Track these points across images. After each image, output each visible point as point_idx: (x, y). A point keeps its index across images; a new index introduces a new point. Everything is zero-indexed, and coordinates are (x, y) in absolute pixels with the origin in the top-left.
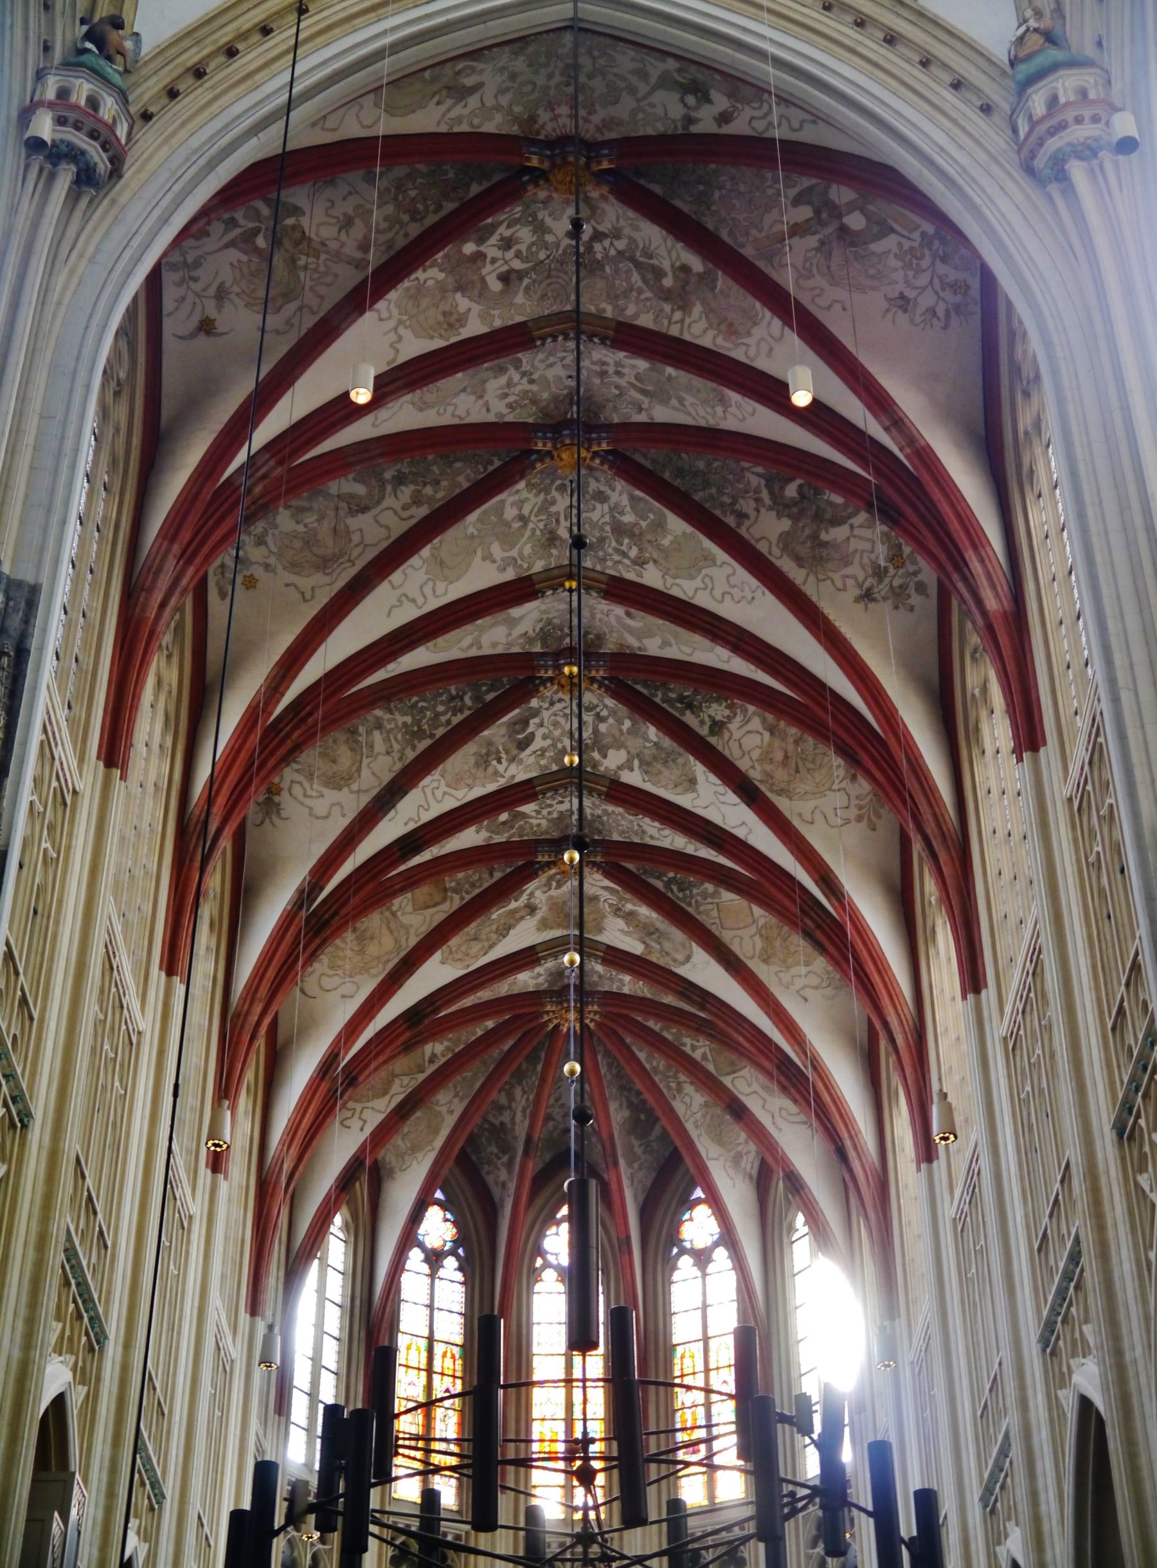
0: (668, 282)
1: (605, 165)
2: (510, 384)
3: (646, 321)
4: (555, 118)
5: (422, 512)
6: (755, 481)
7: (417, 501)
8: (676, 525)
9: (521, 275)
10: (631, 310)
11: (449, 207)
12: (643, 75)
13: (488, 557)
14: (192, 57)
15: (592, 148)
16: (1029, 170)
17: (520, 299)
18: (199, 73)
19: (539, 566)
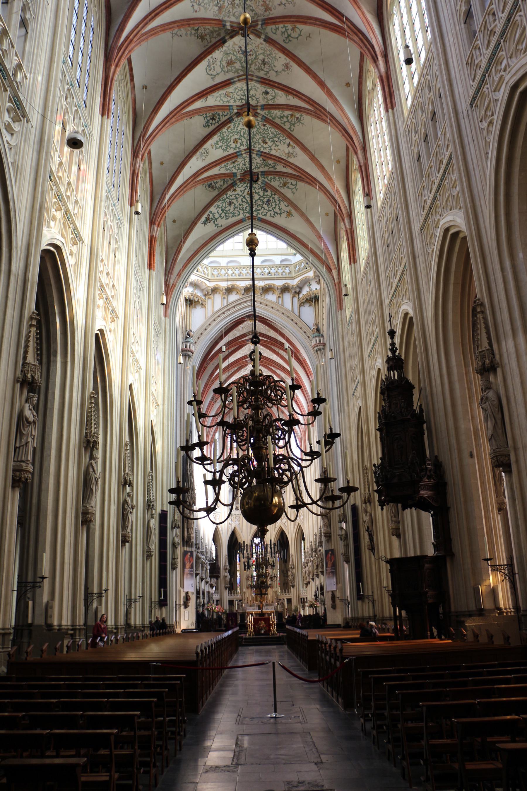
3: (264, 332)
14: (200, 332)
17: (245, 330)
18: (202, 334)
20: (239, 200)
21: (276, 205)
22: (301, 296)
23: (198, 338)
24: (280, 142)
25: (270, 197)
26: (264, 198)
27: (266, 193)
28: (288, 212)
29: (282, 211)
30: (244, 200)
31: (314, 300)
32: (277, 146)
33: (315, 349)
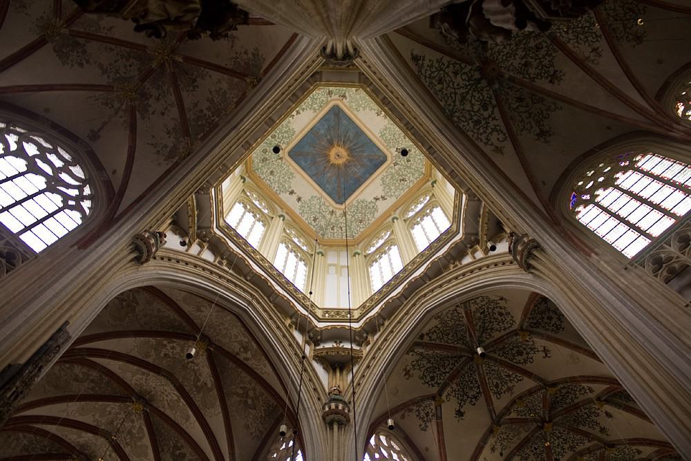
0: (199, 384)
1: (212, 349)
2: (141, 379)
3: (187, 389)
4: (208, 331)
5: (92, 392)
6: (171, 444)
7: (93, 389)
8: (147, 441)
9: (169, 357)
10: (186, 384)
11: (171, 330)
12: (236, 337)
13: (94, 416)
15: (211, 343)
16: (324, 418)
18: (170, 259)
19: (103, 427)
20: (450, 90)
21: (485, 132)
22: (317, 348)
23: (162, 259)
24: (585, 42)
25: (484, 119)
26: (476, 115)
27: (482, 112)
28: (497, 147)
29: (490, 143)
30: (453, 95)
31: (336, 364)
32: (579, 43)
33: (328, 419)
